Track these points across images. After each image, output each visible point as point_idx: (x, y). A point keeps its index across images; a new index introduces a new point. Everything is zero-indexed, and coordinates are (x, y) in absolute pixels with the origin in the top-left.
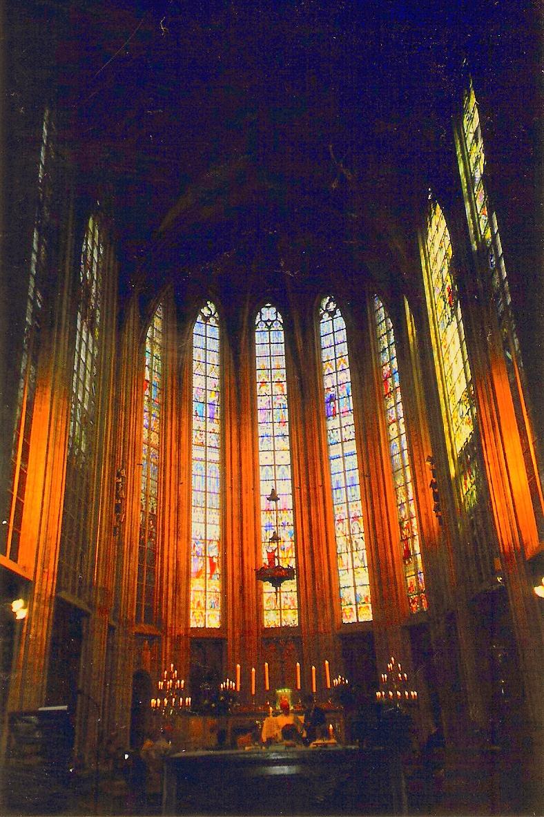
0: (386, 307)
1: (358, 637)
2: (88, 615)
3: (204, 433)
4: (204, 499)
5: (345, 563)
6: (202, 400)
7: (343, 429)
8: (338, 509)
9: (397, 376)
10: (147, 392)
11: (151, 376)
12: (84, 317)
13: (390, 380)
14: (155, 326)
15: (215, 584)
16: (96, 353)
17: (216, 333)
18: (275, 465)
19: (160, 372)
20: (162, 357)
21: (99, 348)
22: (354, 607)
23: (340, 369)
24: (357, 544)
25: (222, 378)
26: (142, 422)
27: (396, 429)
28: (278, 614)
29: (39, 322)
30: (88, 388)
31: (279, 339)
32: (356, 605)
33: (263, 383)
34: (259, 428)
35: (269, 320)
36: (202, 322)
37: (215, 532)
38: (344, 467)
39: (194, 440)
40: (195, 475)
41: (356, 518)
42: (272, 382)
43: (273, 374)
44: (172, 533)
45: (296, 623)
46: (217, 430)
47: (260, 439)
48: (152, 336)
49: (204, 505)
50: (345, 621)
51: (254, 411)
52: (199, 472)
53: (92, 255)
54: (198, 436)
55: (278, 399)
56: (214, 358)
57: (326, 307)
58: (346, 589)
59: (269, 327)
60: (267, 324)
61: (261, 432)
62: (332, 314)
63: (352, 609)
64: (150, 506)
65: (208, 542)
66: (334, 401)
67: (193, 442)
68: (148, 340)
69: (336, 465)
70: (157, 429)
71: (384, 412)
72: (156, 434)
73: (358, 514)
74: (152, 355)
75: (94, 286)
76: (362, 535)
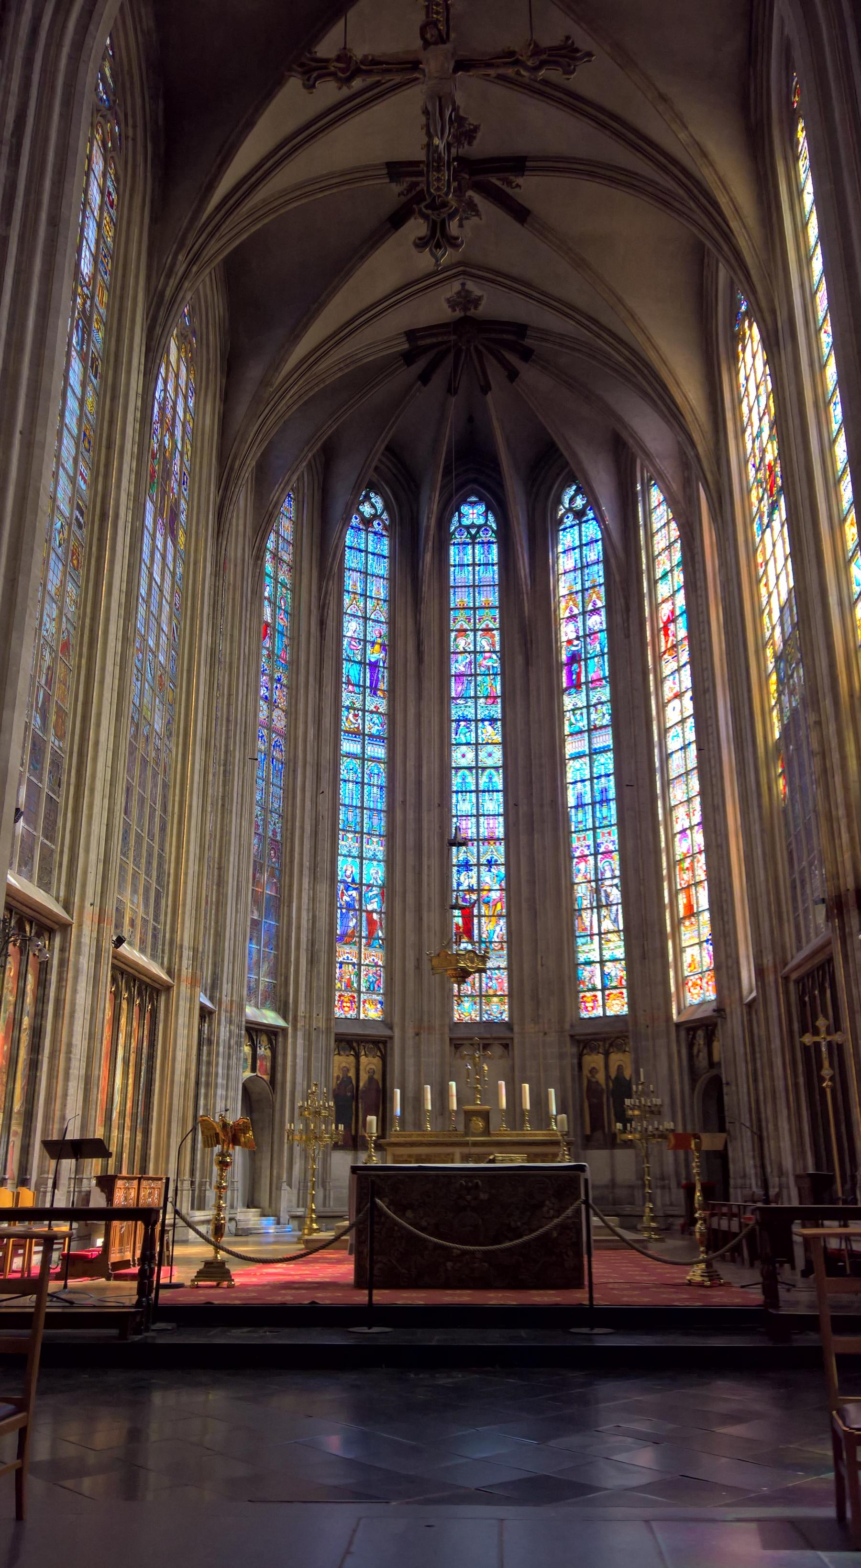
0: (670, 501)
2: (168, 988)
3: (360, 713)
4: (359, 820)
5: (588, 924)
6: (358, 658)
7: (592, 709)
8: (579, 839)
9: (682, 622)
10: (267, 643)
11: (274, 616)
12: (158, 512)
13: (672, 627)
14: (281, 532)
15: (375, 956)
16: (179, 571)
17: (384, 547)
18: (477, 767)
19: (289, 610)
20: (293, 584)
21: (186, 564)
22: (599, 994)
23: (590, 607)
24: (607, 896)
25: (392, 622)
26: (257, 691)
27: (678, 708)
28: (475, 1003)
29: (82, 513)
30: (165, 628)
31: (490, 556)
32: (604, 988)
33: (462, 631)
34: (453, 705)
35: (473, 525)
36: (361, 526)
38: (591, 772)
39: (345, 725)
40: (345, 781)
41: (608, 853)
42: (475, 630)
43: (477, 617)
44: (306, 872)
45: (505, 1017)
47: (454, 725)
48: (277, 549)
49: (358, 829)
50: (584, 1015)
51: (444, 676)
52: (351, 776)
53: (174, 408)
54: (351, 716)
55: (485, 658)
56: (379, 589)
57: (570, 503)
58: (588, 968)
59: (473, 537)
60: (469, 533)
61: (455, 713)
62: (580, 515)
63: (595, 996)
64: (271, 827)
65: (364, 888)
66: (579, 662)
67: (343, 728)
68: (268, 556)
69: (575, 770)
70: (283, 703)
72: (280, 712)
73: (612, 848)
74: (276, 580)
75: (177, 460)
76: (616, 881)
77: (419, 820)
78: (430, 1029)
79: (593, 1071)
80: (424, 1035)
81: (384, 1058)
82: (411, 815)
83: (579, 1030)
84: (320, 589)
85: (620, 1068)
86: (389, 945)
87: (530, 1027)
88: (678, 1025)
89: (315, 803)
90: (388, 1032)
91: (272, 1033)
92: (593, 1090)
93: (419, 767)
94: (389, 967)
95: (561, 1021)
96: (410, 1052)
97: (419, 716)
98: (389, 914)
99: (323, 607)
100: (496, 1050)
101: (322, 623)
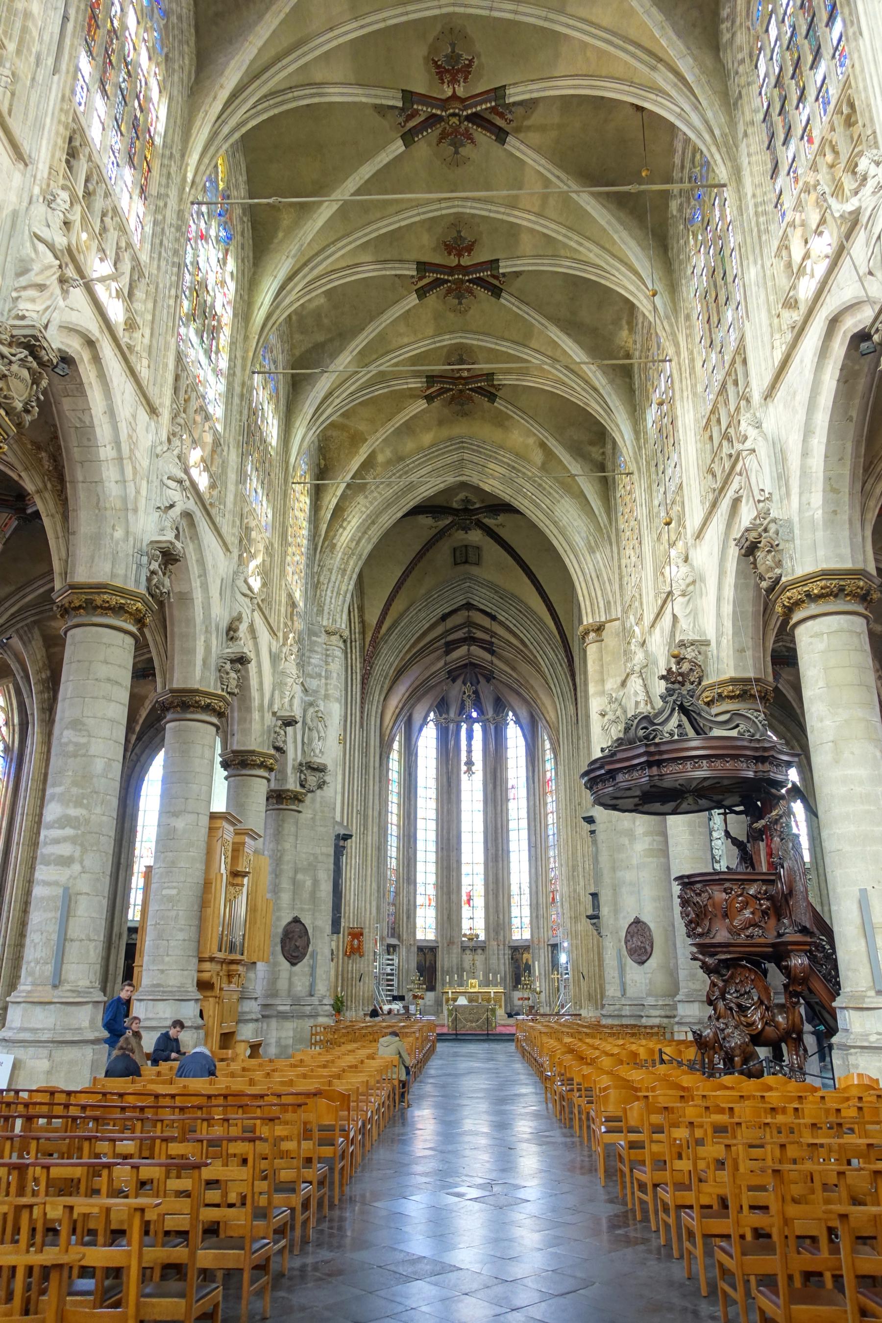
1: (517, 951)
15: (431, 913)
37: (432, 879)
39: (419, 816)
71: (546, 804)
77: (449, 856)
83: (512, 944)
86: (437, 907)
91: (394, 947)
94: (436, 918)
97: (448, 811)
98: (437, 896)
100: (479, 951)
101: (410, 774)
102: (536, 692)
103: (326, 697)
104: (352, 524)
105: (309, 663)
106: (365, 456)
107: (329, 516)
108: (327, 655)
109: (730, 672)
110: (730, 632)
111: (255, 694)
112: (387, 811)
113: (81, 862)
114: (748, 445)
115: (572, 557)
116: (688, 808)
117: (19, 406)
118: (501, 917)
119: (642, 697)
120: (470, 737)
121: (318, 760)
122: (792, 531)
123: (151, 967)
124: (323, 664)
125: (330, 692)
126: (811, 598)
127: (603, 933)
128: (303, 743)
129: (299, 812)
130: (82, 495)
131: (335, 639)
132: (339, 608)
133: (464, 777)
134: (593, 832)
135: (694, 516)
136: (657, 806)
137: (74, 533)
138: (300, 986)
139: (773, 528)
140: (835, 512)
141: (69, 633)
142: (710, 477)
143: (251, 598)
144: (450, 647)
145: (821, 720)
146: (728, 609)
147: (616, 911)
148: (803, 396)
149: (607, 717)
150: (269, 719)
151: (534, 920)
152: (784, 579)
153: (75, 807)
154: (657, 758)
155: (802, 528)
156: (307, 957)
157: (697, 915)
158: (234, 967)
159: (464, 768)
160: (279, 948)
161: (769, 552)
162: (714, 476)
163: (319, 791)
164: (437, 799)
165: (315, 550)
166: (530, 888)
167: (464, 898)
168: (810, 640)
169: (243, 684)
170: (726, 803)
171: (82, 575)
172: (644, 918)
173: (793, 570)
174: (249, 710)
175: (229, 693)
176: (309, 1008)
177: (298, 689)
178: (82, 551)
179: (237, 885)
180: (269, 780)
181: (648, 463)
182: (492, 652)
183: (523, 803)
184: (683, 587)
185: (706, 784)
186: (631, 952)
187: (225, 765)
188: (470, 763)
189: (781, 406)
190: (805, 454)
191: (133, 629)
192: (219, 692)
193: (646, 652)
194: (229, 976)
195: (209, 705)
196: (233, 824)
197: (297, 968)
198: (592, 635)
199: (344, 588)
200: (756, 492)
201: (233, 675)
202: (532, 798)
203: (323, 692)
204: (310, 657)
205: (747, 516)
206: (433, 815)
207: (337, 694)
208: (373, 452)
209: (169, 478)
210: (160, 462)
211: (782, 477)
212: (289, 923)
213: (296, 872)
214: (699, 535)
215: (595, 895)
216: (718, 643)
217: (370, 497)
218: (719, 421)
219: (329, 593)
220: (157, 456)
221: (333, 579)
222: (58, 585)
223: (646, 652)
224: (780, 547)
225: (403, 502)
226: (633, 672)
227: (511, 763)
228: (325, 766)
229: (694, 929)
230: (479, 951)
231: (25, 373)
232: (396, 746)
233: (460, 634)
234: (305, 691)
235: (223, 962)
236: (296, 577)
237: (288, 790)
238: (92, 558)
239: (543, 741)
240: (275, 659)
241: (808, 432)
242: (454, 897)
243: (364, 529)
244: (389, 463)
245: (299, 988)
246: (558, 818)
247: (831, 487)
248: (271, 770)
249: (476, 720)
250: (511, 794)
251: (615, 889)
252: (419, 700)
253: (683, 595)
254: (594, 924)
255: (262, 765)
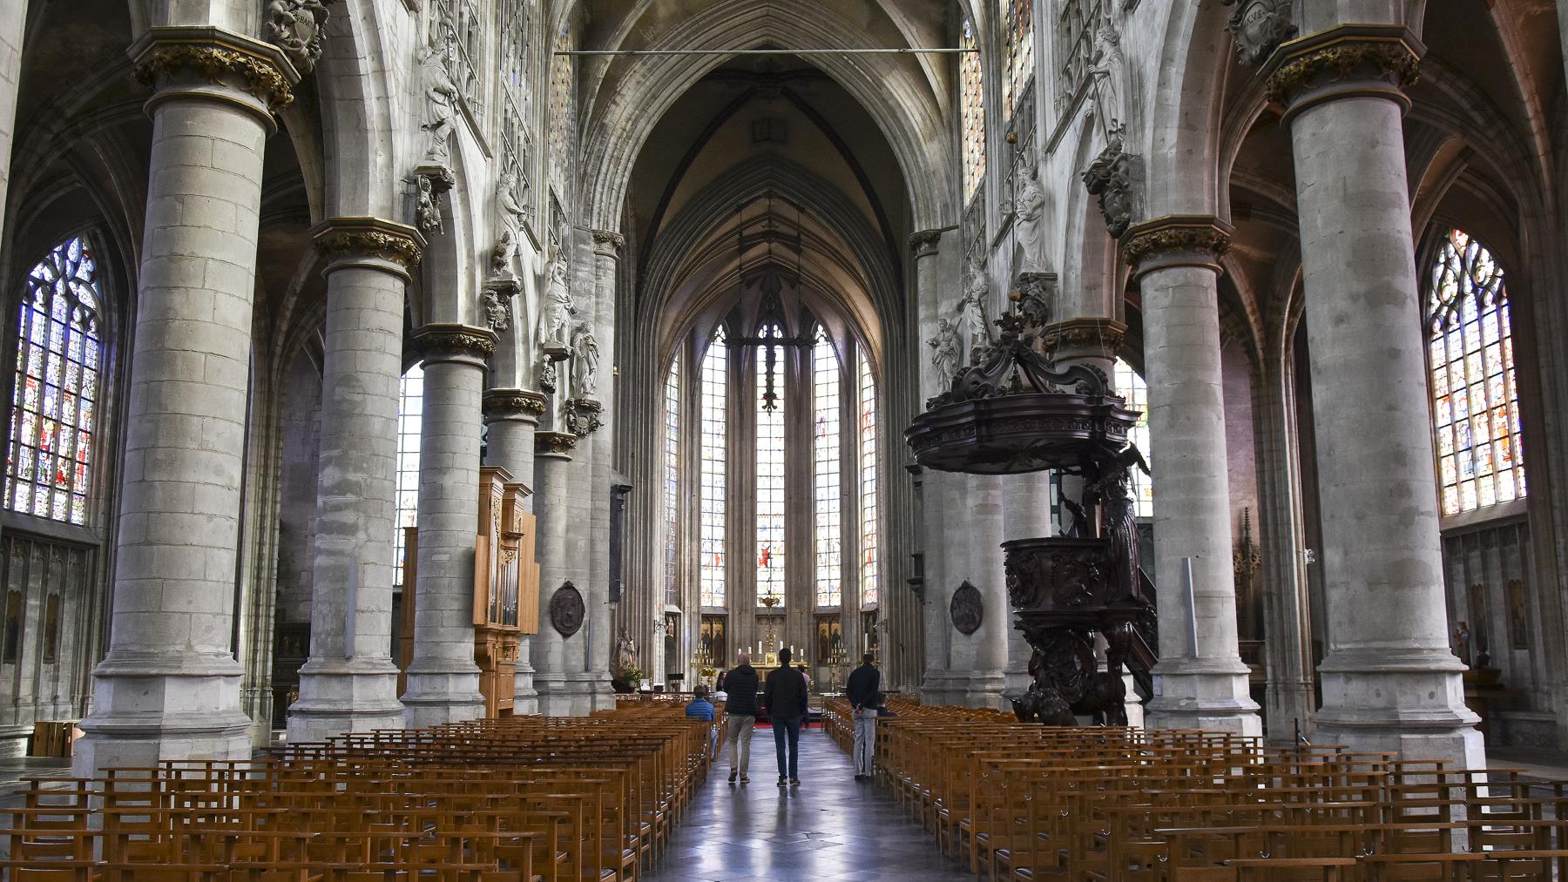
15: (720, 574)
37: (720, 533)
46: (723, 445)
50: (820, 604)
77: (741, 506)
78: (746, 610)
79: (824, 631)
80: (743, 613)
81: (724, 625)
82: (737, 503)
84: (691, 385)
85: (836, 630)
86: (726, 568)
87: (794, 610)
88: (862, 613)
89: (691, 501)
90: (725, 613)
92: (823, 639)
93: (741, 477)
95: (809, 608)
96: (736, 622)
97: (741, 448)
98: (726, 554)
99: (693, 395)
100: (778, 621)
101: (692, 405)
102: (853, 303)
103: (598, 319)
104: (628, 98)
105: (576, 277)
106: (644, 10)
107: (598, 87)
108: (598, 267)
109: (1078, 314)
110: (1080, 266)
111: (518, 323)
112: (664, 451)
113: (366, 530)
114: (1102, 65)
115: (903, 144)
116: (1021, 468)
117: (305, 51)
118: (805, 580)
119: (979, 329)
120: (771, 361)
121: (590, 397)
122: (1143, 170)
123: (425, 639)
124: (593, 278)
125: (602, 313)
126: (1157, 247)
127: (928, 599)
128: (571, 377)
129: (568, 460)
130: (340, 115)
131: (607, 248)
132: (612, 207)
133: (762, 417)
134: (918, 484)
135: (1047, 119)
136: (987, 466)
137: (330, 158)
138: (577, 661)
139: (1123, 166)
140: (1190, 152)
141: (330, 277)
142: (1066, 78)
143: (519, 215)
144: (744, 245)
145: (1160, 382)
146: (1078, 239)
147: (942, 575)
148: (1161, 19)
149: (938, 349)
150: (534, 353)
151: (846, 584)
152: (1131, 225)
153: (355, 471)
154: (986, 417)
155: (1154, 168)
156: (581, 628)
157: (1023, 585)
158: (510, 639)
159: (761, 403)
160: (548, 619)
161: (1117, 193)
162: (1070, 79)
163: (590, 438)
164: (727, 435)
165: (581, 132)
166: (842, 544)
167: (760, 556)
168: (1156, 294)
169: (509, 320)
170: (1062, 462)
171: (345, 212)
172: (975, 583)
173: (1142, 214)
174: (511, 342)
175: (495, 329)
176: (586, 685)
177: (566, 316)
178: (344, 182)
179: (510, 548)
180: (535, 425)
181: (998, 40)
182: (798, 252)
183: (835, 441)
184: (1029, 211)
185: (1040, 444)
186: (957, 622)
187: (487, 408)
188: (770, 396)
189: (1141, 21)
190: (1162, 83)
191: (402, 269)
192: (486, 329)
193: (987, 275)
194: (505, 648)
195: (475, 343)
196: (502, 479)
197: (571, 640)
198: (924, 247)
199: (618, 181)
200: (1108, 122)
201: (500, 308)
202: (845, 435)
203: (593, 313)
204: (576, 270)
205: (1097, 148)
206: (720, 454)
207: (611, 315)
208: (654, 4)
209: (435, 90)
210: (425, 70)
211: (1135, 106)
212: (560, 589)
213: (567, 530)
214: (1051, 148)
215: (919, 558)
216: (1066, 278)
217: (649, 63)
218: (1079, 12)
219: (599, 189)
220: (420, 62)
221: (604, 169)
222: (314, 219)
223: (987, 275)
224: (1130, 189)
225: (690, 71)
226: (970, 299)
227: (820, 391)
228: (598, 404)
229: (1019, 597)
230: (778, 621)
231: (310, 15)
232: (674, 368)
233: (758, 228)
234: (572, 312)
235: (498, 633)
236: (559, 169)
237: (555, 434)
238: (355, 188)
239: (861, 364)
240: (540, 281)
241: (1166, 59)
242: (746, 556)
243: (643, 106)
244: (674, 19)
245: (574, 663)
246: (878, 460)
247: (1189, 123)
248: (537, 412)
249: (779, 342)
250: (819, 431)
251: (942, 549)
252: (704, 309)
253: (1029, 220)
254: (916, 590)
255: (529, 409)
